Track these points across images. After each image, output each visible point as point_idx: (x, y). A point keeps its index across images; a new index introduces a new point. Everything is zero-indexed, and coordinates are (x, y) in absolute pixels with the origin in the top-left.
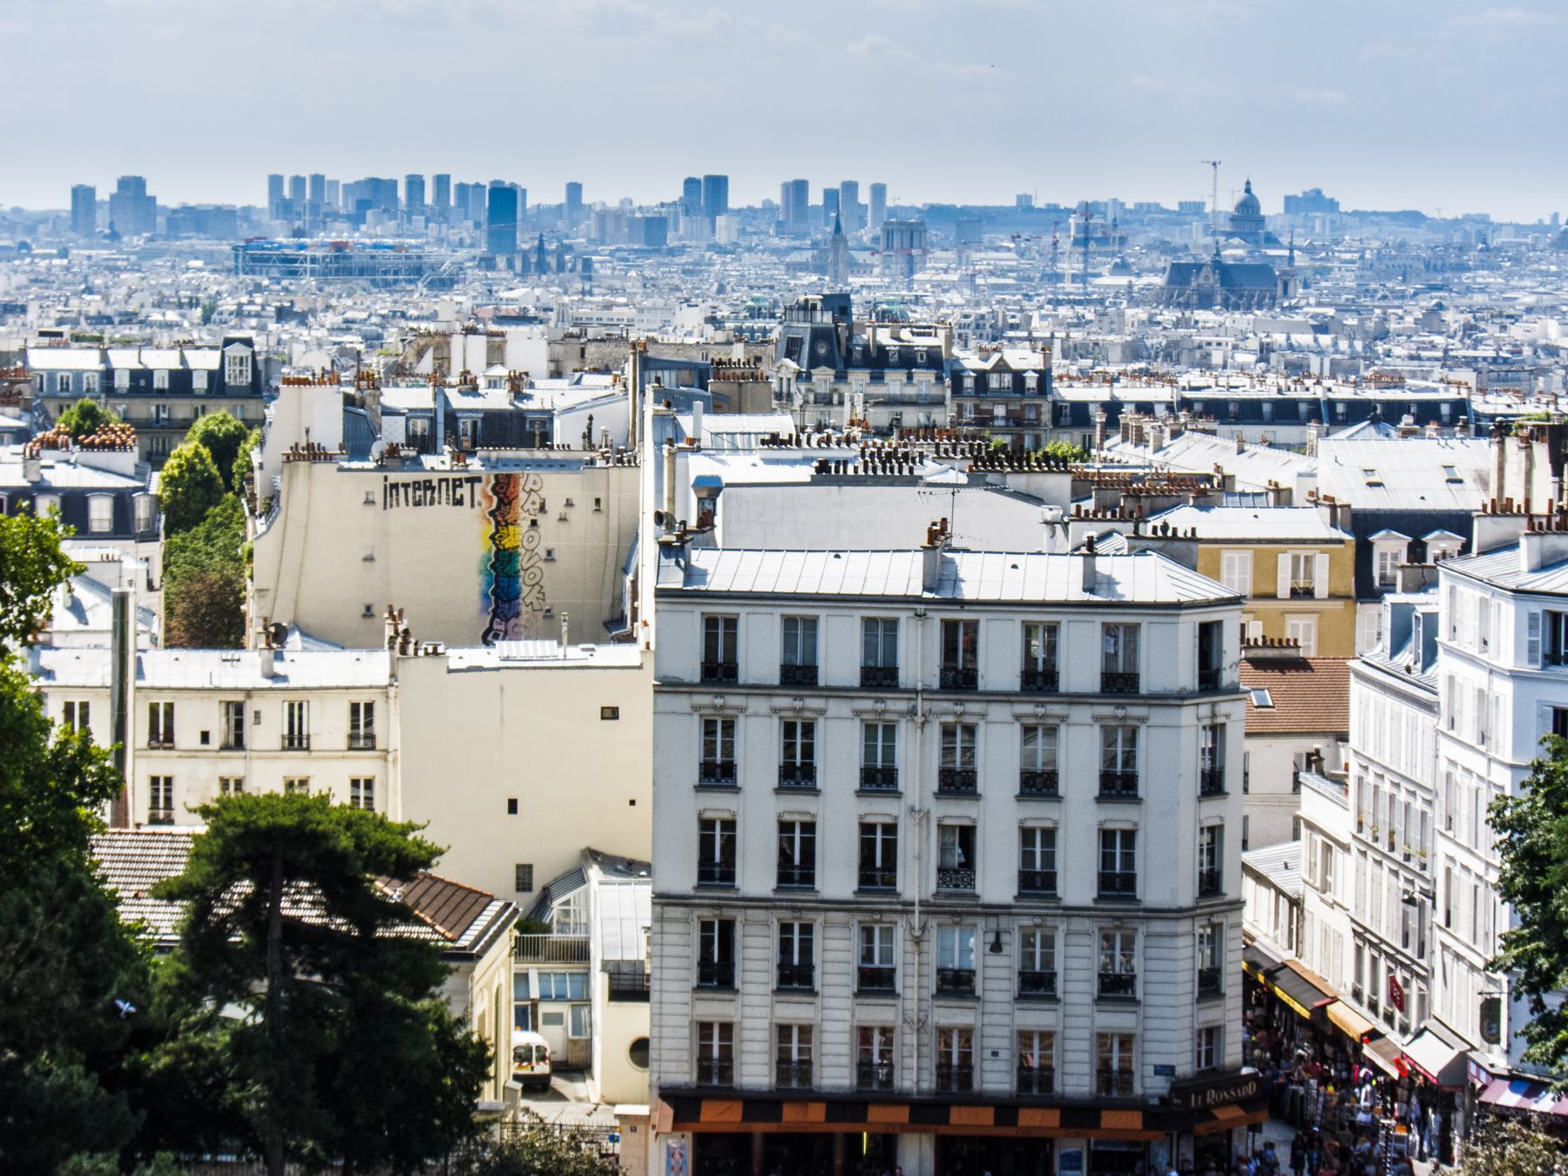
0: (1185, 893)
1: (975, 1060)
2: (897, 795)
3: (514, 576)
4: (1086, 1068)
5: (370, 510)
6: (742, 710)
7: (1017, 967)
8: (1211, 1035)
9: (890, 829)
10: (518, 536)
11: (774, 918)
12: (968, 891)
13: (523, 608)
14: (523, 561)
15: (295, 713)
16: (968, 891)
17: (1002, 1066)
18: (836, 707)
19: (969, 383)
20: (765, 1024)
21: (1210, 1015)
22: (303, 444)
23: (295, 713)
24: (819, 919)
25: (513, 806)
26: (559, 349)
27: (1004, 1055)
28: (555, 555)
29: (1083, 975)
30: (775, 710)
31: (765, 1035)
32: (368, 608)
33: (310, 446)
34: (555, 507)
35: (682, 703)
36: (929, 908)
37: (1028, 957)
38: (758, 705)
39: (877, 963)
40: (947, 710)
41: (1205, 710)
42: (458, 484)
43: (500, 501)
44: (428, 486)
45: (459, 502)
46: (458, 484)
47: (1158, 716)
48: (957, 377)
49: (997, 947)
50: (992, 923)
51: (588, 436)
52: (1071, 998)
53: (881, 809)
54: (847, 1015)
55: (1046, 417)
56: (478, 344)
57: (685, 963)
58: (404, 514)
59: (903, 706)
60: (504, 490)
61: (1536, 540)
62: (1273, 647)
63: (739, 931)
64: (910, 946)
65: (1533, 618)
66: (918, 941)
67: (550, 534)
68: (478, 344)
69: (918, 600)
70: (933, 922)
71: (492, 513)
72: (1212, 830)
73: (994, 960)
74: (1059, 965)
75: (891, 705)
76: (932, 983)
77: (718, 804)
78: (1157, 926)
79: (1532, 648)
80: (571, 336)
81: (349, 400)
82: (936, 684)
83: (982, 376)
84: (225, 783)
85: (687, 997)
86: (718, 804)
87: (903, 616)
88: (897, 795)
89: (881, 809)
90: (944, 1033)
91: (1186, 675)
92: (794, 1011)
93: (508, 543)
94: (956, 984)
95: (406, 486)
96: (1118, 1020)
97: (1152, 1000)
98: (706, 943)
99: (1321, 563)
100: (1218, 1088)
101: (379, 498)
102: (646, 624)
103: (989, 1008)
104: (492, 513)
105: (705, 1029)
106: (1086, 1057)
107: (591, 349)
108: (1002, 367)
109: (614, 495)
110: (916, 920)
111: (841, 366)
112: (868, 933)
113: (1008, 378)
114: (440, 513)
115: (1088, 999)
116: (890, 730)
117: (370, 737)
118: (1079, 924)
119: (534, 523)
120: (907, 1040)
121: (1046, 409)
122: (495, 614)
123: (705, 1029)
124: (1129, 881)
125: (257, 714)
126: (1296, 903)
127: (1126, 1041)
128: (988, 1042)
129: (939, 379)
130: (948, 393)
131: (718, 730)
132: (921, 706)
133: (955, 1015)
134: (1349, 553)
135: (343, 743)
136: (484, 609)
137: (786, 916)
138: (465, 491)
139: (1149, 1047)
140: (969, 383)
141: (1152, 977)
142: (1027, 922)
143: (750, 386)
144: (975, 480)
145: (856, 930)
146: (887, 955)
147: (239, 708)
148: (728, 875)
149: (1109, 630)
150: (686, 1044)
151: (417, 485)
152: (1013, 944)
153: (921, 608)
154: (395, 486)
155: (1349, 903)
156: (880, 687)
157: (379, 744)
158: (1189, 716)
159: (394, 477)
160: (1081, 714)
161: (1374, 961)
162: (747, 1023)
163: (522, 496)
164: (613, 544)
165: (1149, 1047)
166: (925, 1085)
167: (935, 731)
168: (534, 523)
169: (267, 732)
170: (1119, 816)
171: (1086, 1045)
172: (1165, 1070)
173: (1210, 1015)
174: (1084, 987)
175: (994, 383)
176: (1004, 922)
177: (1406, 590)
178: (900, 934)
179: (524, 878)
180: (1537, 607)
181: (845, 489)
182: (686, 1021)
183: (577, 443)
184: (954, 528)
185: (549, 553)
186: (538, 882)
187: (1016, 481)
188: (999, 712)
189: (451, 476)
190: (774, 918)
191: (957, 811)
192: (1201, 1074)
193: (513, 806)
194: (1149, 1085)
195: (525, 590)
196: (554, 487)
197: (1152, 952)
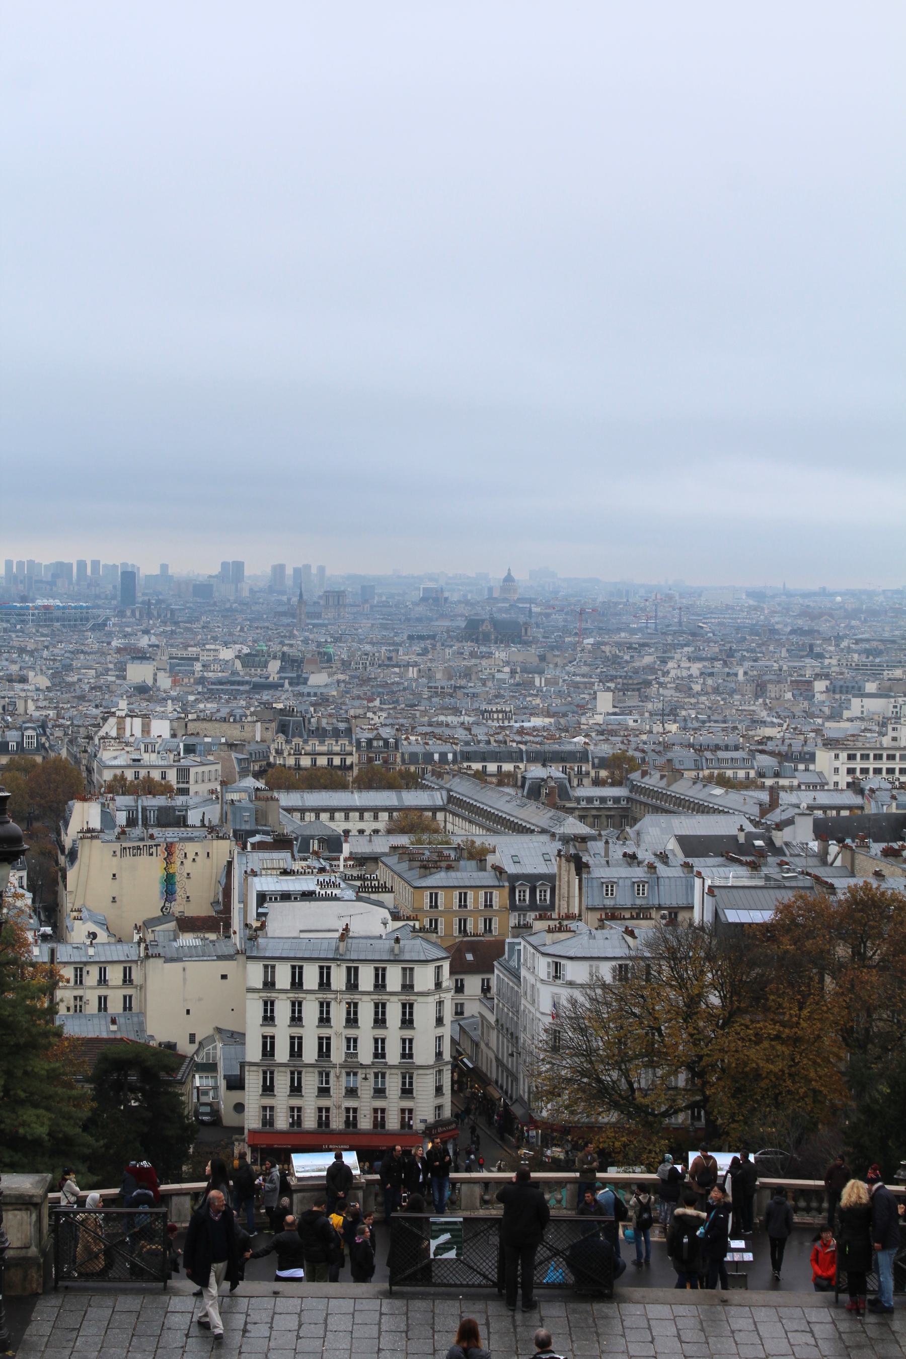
0: (431, 1060)
1: (358, 1118)
2: (331, 1027)
3: (174, 884)
4: (396, 1121)
5: (115, 858)
6: (277, 998)
7: (373, 1086)
8: (439, 1108)
9: (329, 1039)
10: (176, 868)
11: (288, 1070)
12: (355, 1060)
13: (178, 898)
14: (177, 878)
15: (102, 972)
16: (355, 1060)
17: (368, 1120)
18: (309, 997)
19: (364, 744)
20: (285, 1107)
21: (439, 1101)
22: (85, 828)
23: (102, 972)
24: (304, 1070)
25: (188, 1012)
26: (175, 724)
27: (368, 1116)
28: (191, 875)
29: (395, 1088)
30: (288, 998)
31: (285, 1110)
32: (114, 898)
33: (89, 831)
34: (191, 856)
35: (256, 995)
36: (342, 1066)
37: (376, 1083)
38: (283, 996)
39: (324, 1085)
40: (348, 997)
41: (437, 997)
42: (151, 847)
43: (168, 854)
44: (139, 848)
45: (151, 854)
46: (151, 847)
47: (420, 999)
48: (358, 742)
49: (366, 1079)
50: (364, 1071)
51: (203, 821)
52: (391, 1097)
53: (325, 1032)
54: (313, 1103)
55: (399, 760)
56: (138, 722)
57: (256, 1085)
58: (129, 860)
59: (333, 996)
60: (170, 849)
61: (551, 934)
62: (474, 936)
63: (276, 1074)
64: (335, 1079)
65: (549, 963)
66: (338, 1077)
67: (188, 866)
68: (138, 722)
69: (338, 960)
70: (344, 1071)
71: (165, 859)
72: (440, 1037)
73: (366, 1083)
74: (387, 1086)
75: (329, 996)
76: (343, 1091)
77: (269, 1031)
78: (421, 1072)
79: (549, 973)
80: (180, 718)
81: (103, 805)
82: (344, 989)
83: (370, 741)
84: (75, 998)
85: (258, 1097)
86: (269, 1031)
87: (333, 966)
88: (331, 1027)
89: (325, 1032)
90: (348, 1110)
91: (432, 986)
92: (295, 1102)
93: (171, 871)
94: (352, 1092)
95: (129, 848)
96: (407, 1104)
97: (419, 1097)
98: (265, 1079)
99: (496, 893)
100: (442, 1126)
101: (118, 853)
102: (235, 933)
103: (363, 1100)
104: (165, 859)
105: (264, 1108)
106: (396, 1117)
107: (190, 725)
108: (378, 737)
109: (215, 851)
110: (338, 1070)
111: (306, 737)
112: (320, 1073)
113: (381, 743)
114: (143, 860)
115: (397, 1097)
116: (328, 1005)
117: (131, 981)
118: (393, 1071)
119: (182, 862)
120: (333, 1113)
121: (399, 755)
122: (166, 900)
123: (264, 1108)
124: (411, 1056)
125: (88, 972)
126: (477, 1045)
127: (411, 1111)
128: (362, 1112)
129: (351, 743)
130: (354, 749)
131: (269, 1006)
132: (339, 996)
133: (351, 1103)
134: (507, 890)
135: (120, 982)
136: (162, 898)
137: (293, 1069)
138: (154, 850)
139: (418, 1113)
140: (364, 744)
141: (419, 1089)
142: (376, 1070)
143: (271, 803)
144: (359, 899)
145: (317, 1073)
146: (327, 1082)
147: (81, 969)
148: (272, 1054)
149: (404, 969)
150: (257, 1114)
151: (134, 848)
152: (371, 1077)
153: (339, 963)
154: (125, 848)
155: (495, 1049)
156: (325, 990)
157: (135, 983)
158: (432, 1000)
159: (124, 845)
160: (394, 999)
161: (502, 1072)
162: (279, 1106)
163: (177, 852)
164: (215, 871)
165: (418, 1113)
166: (341, 1127)
167: (344, 1006)
168: (182, 862)
169: (92, 978)
170: (407, 1034)
171: (396, 1113)
172: (424, 1121)
173: (439, 1101)
174: (396, 1092)
175: (375, 743)
176: (368, 1071)
177: (514, 937)
178: (332, 1076)
179: (192, 1039)
180: (550, 960)
181: (312, 903)
182: (257, 1106)
183: (198, 824)
184: (351, 928)
185: (188, 874)
186: (198, 1039)
187: (374, 896)
188: (366, 998)
189: (148, 844)
190: (288, 1070)
191: (351, 1033)
192: (436, 1122)
193: (188, 1012)
194: (418, 1126)
195: (178, 890)
196: (190, 848)
197: (419, 1080)
